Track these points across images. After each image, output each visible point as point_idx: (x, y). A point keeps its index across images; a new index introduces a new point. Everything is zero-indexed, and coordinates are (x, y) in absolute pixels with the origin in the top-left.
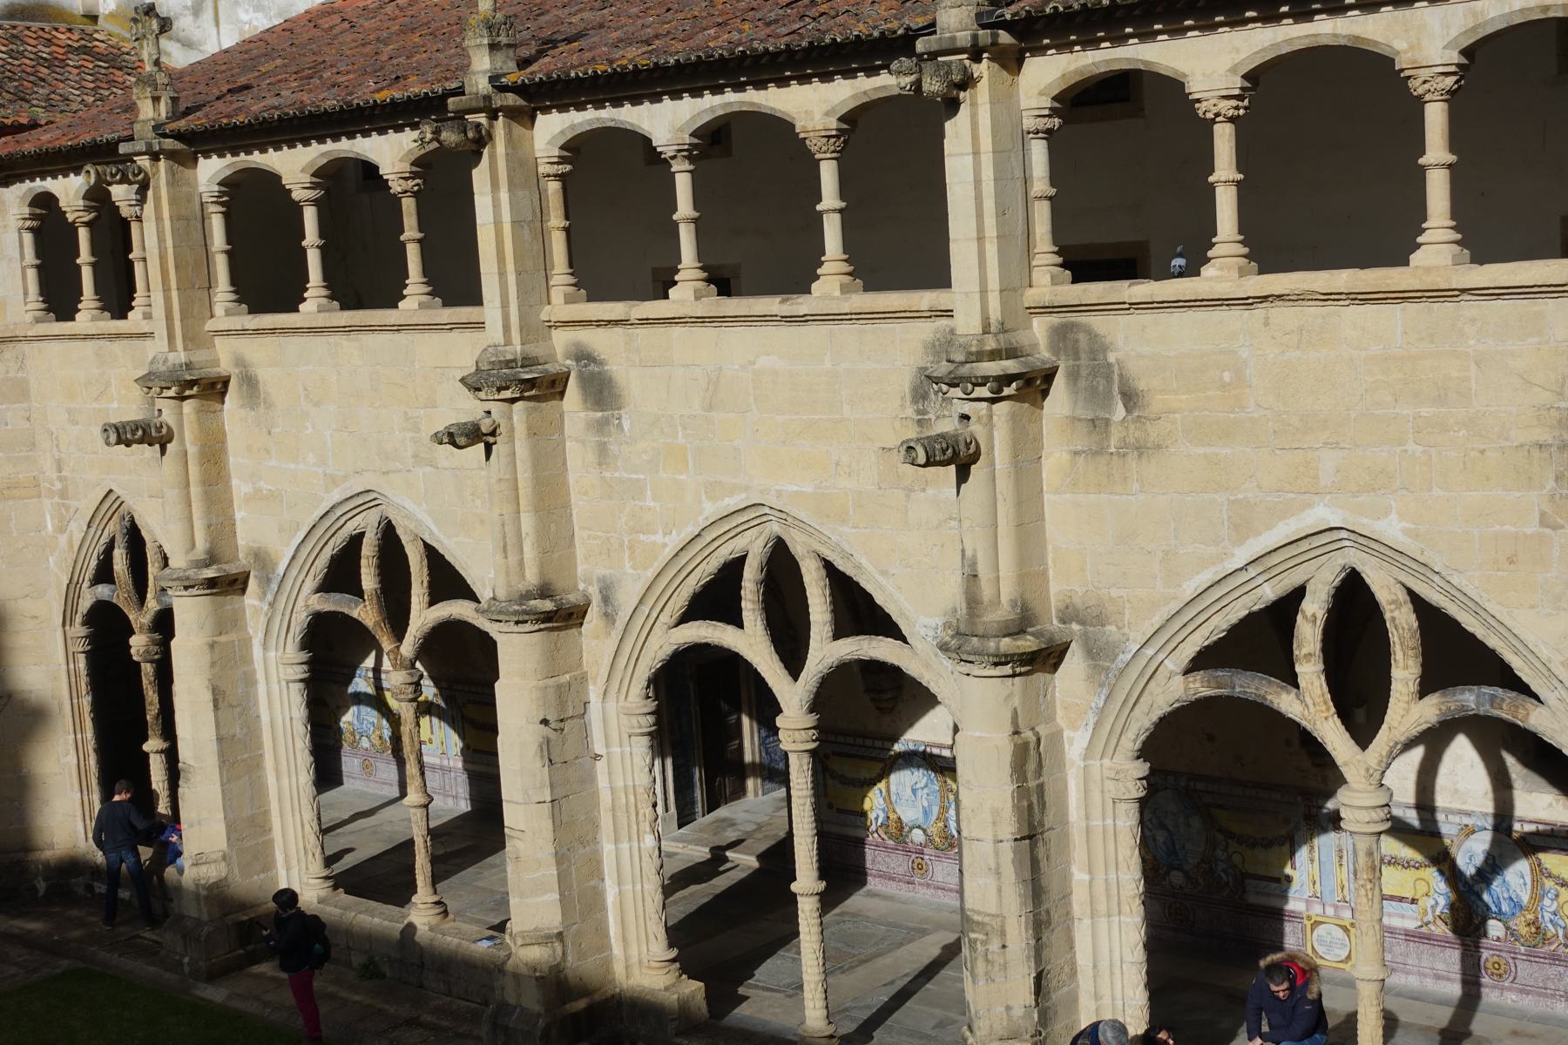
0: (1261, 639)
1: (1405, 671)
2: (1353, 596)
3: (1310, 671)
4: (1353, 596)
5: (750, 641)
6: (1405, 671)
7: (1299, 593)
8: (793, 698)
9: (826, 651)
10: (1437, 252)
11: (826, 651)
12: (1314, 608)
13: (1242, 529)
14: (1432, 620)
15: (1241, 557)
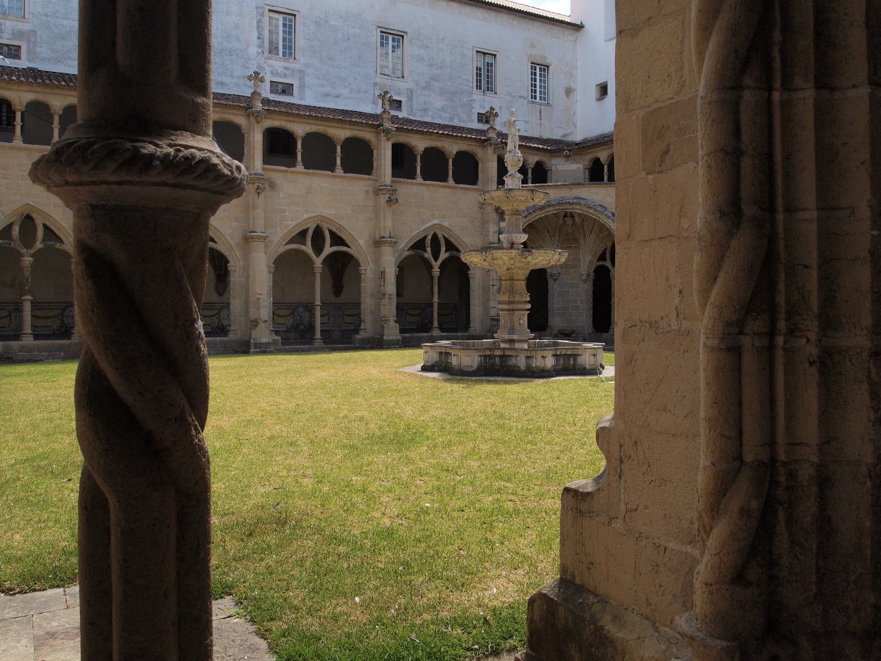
0: (419, 245)
1: (443, 249)
2: (435, 237)
3: (429, 249)
4: (435, 237)
5: (308, 249)
6: (443, 249)
7: (426, 237)
8: (318, 261)
9: (328, 250)
10: (451, 182)
11: (328, 250)
12: (430, 237)
13: (423, 223)
14: (447, 241)
15: (423, 228)
